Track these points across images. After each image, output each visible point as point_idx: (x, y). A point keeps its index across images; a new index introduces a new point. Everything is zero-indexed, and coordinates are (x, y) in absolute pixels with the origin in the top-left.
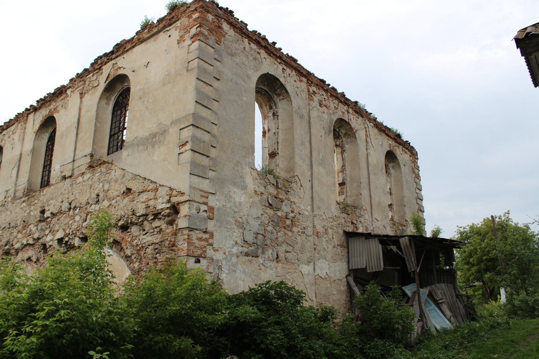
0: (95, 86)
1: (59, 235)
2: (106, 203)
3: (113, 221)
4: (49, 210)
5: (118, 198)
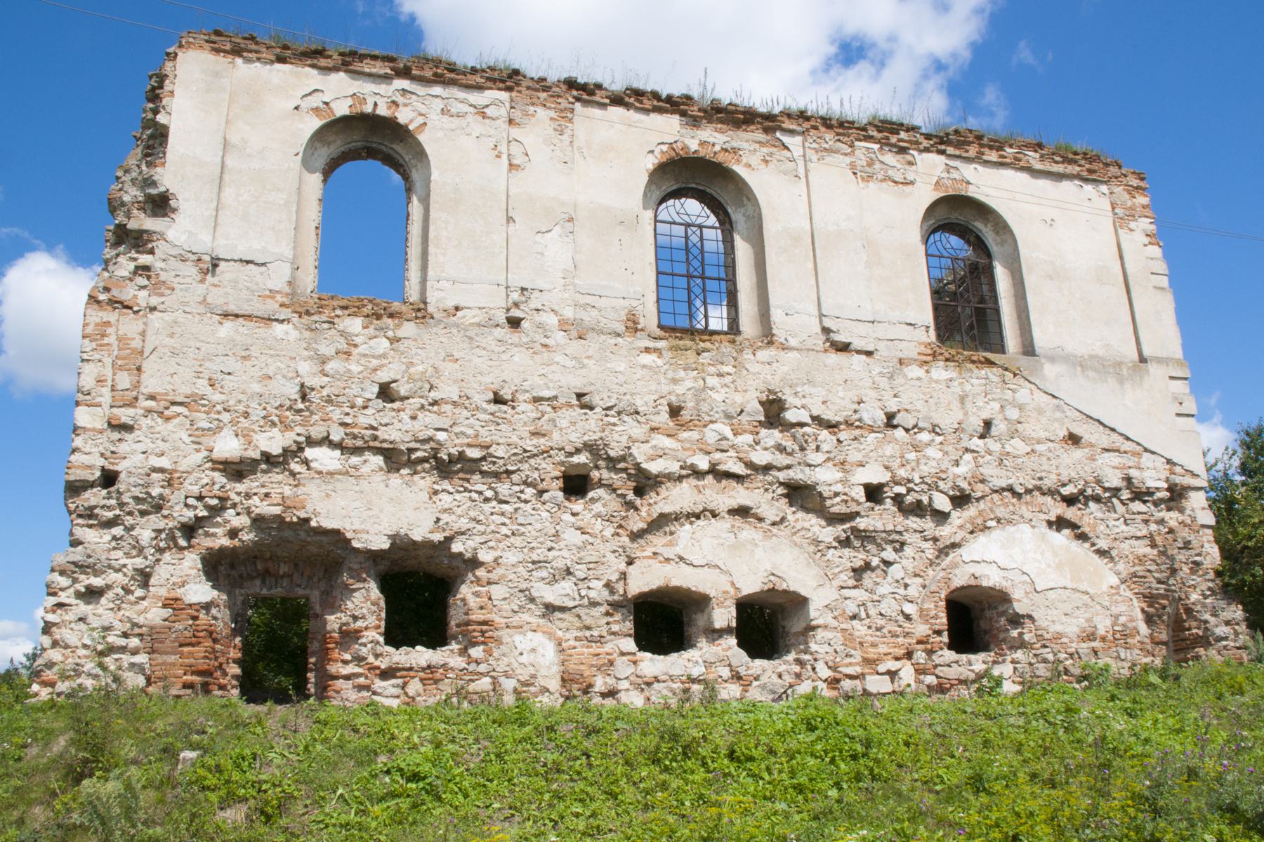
0: (897, 179)
1: (875, 475)
2: (1017, 446)
3: (1048, 483)
5: (1051, 445)
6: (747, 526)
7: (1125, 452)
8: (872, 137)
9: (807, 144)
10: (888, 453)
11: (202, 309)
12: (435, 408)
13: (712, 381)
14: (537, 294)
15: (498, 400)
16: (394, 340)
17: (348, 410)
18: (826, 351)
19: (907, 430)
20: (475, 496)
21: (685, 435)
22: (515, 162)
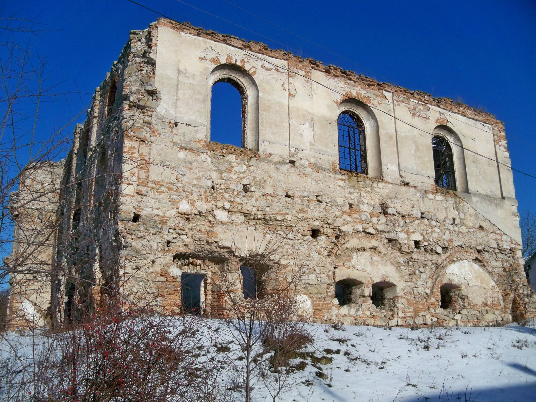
2: (463, 229)
3: (473, 245)
4: (394, 207)
5: (474, 229)
6: (376, 255)
7: (497, 234)
8: (415, 97)
9: (394, 98)
10: (422, 228)
11: (172, 144)
12: (264, 197)
13: (363, 194)
14: (300, 151)
15: (287, 196)
16: (248, 166)
17: (231, 195)
18: (401, 185)
19: (428, 220)
20: (278, 236)
21: (354, 216)
22: (292, 93)
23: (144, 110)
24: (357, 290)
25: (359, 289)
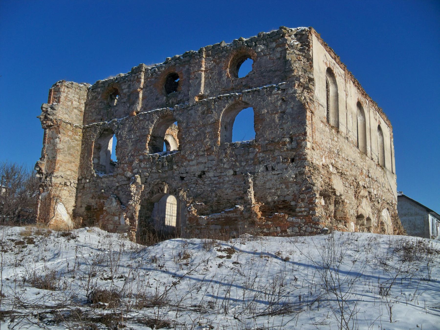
1: (375, 193)
15: (347, 160)
16: (338, 138)
23: (309, 91)
24: (359, 221)
25: (360, 220)
